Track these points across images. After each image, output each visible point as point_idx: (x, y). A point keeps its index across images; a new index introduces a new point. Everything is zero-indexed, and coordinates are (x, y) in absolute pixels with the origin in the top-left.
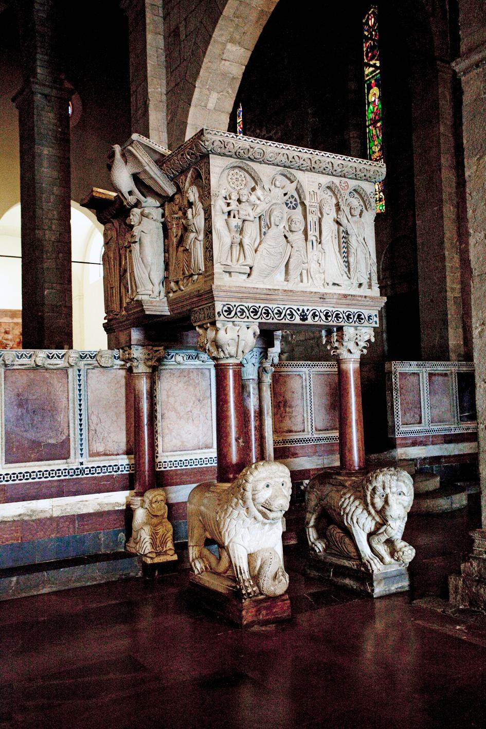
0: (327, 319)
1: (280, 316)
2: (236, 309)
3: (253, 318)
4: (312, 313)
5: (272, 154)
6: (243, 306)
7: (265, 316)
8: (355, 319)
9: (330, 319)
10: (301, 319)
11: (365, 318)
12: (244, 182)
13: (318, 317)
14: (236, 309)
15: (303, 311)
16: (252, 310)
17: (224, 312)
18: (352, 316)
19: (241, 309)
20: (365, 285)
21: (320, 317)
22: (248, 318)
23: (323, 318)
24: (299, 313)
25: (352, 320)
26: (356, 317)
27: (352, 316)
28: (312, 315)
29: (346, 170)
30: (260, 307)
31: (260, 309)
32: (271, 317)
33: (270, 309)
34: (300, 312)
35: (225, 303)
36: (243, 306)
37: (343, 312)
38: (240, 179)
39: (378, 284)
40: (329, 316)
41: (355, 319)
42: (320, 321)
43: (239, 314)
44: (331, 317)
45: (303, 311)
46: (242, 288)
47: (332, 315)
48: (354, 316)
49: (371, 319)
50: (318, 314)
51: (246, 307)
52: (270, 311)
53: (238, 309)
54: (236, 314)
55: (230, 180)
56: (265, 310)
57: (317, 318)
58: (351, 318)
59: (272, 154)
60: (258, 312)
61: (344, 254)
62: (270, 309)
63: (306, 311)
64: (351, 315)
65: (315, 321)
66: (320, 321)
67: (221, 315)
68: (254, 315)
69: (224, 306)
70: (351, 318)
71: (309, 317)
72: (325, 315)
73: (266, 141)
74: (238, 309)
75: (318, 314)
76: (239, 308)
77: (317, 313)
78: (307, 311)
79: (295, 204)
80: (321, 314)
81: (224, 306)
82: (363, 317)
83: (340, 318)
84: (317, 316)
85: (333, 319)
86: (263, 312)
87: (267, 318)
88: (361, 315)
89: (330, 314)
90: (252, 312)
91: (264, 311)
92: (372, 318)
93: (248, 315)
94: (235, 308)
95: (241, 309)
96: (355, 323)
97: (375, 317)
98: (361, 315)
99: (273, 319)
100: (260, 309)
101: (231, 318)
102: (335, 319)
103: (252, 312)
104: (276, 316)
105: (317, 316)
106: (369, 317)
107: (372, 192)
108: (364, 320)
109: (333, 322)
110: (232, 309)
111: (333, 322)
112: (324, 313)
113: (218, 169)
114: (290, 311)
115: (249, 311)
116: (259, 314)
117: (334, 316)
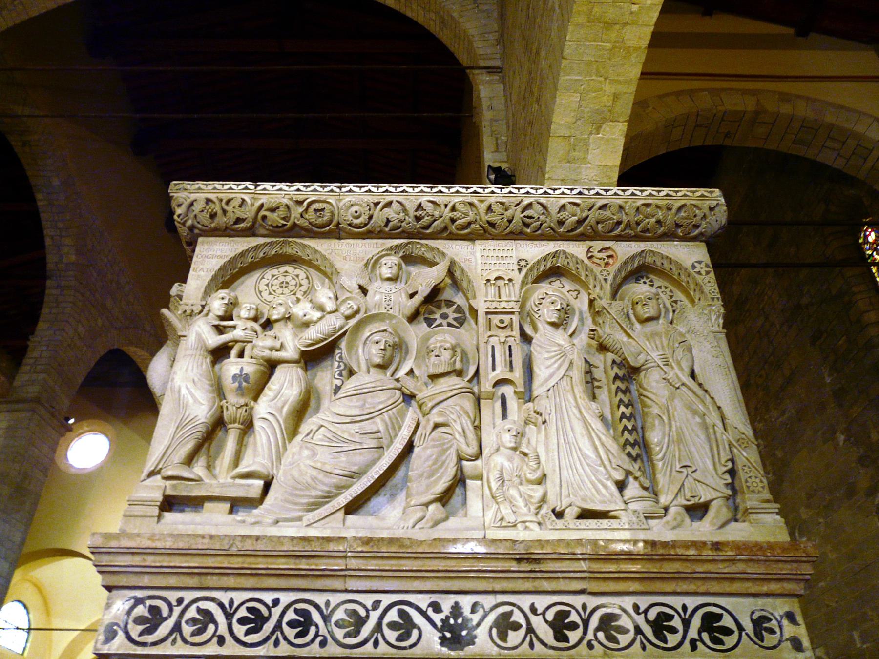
0: (560, 636)
1: (357, 633)
2: (183, 612)
3: (244, 644)
4: (492, 617)
5: (354, 209)
6: (212, 600)
7: (290, 633)
8: (693, 633)
9: (574, 636)
10: (444, 641)
11: (741, 628)
12: (304, 289)
13: (523, 631)
14: (183, 612)
15: (456, 610)
16: (242, 613)
17: (131, 626)
18: (677, 623)
19: (199, 610)
20: (718, 511)
21: (530, 630)
22: (221, 641)
23: (546, 633)
24: (437, 618)
25: (679, 636)
26: (696, 622)
27: (677, 623)
28: (497, 624)
29: (594, 215)
30: (276, 602)
31: (277, 612)
32: (317, 635)
33: (317, 607)
34: (442, 616)
35: (140, 594)
36: (212, 600)
37: (636, 608)
38: (282, 279)
39: (776, 501)
40: (573, 626)
41: (693, 633)
42: (532, 645)
43: (187, 630)
44: (580, 631)
45: (456, 610)
46: (200, 540)
47: (586, 623)
48: (686, 623)
49: (772, 631)
50: (522, 621)
51: (221, 605)
52: (316, 617)
53: (192, 613)
54: (177, 628)
55: (262, 287)
56: (296, 611)
57: (514, 638)
58: (673, 631)
59: (354, 209)
60: (267, 619)
61: (624, 420)
62: (317, 607)
63: (466, 611)
64: (671, 618)
65: (509, 645)
66: (532, 645)
67: (114, 634)
68: (247, 633)
69: (138, 602)
70: (673, 631)
71: (482, 633)
72: (551, 624)
73: (339, 185)
74: (192, 613)
75: (522, 621)
76: (194, 607)
77: (517, 617)
78: (473, 611)
79: (455, 319)
80: (537, 622)
81: (138, 602)
82: (727, 622)
83: (624, 631)
84: (516, 627)
85: (590, 636)
86: (286, 619)
87: (299, 641)
88: (719, 617)
89: (574, 617)
90: (242, 621)
91: (291, 615)
92: (774, 624)
93: (223, 629)
94: (177, 611)
95: (199, 610)
96: (694, 647)
97: (785, 622)
98: (719, 617)
99: (323, 644)
100: (277, 612)
101: (155, 644)
102: (601, 635)
103: (242, 621)
104: (339, 633)
105: (516, 627)
106: (760, 623)
107: (700, 262)
108: (735, 637)
109: (590, 646)
110: (165, 613)
111: (590, 646)
112: (550, 616)
113: (215, 261)
114: (402, 613)
115: (229, 616)
116: (268, 627)
117: (594, 622)
